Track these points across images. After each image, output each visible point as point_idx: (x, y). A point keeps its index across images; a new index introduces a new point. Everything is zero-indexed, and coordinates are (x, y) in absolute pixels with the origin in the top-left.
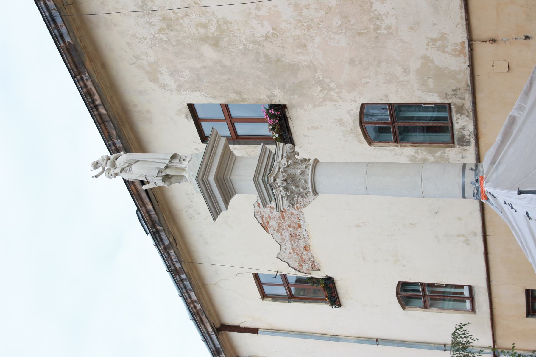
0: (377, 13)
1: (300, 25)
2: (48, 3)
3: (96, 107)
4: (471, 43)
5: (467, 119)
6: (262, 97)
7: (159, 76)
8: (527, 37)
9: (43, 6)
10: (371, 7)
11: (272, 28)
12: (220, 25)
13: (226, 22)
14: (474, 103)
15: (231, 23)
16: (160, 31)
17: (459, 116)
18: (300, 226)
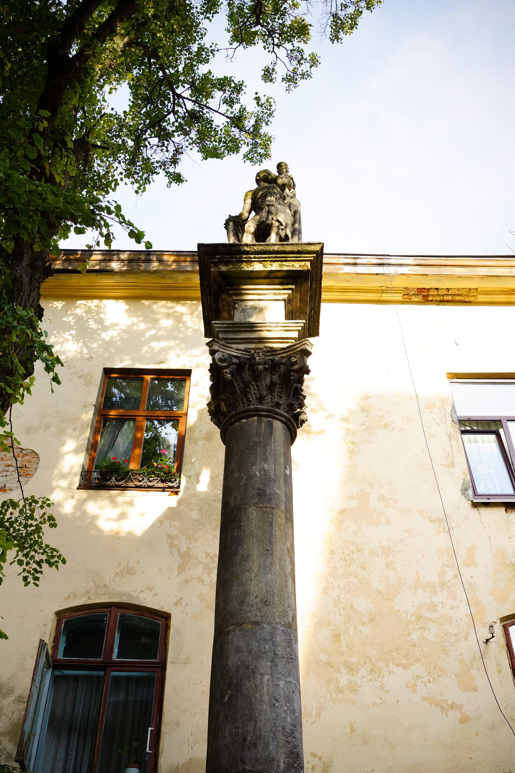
1: (353, 548)
10: (398, 666)
11: (345, 509)
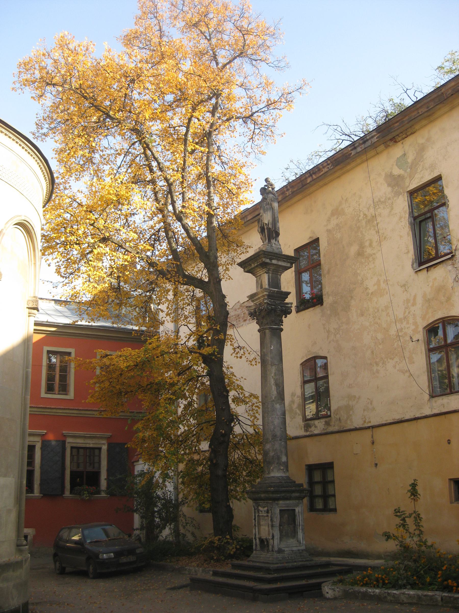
0: (387, 363)
2: (375, 138)
3: (311, 175)
4: (371, 429)
5: (322, 429)
6: (327, 288)
7: (335, 217)
8: (376, 465)
9: (373, 134)
12: (372, 255)
13: (374, 259)
14: (332, 433)
15: (374, 263)
16: (365, 215)
17: (324, 423)
18: (245, 320)
